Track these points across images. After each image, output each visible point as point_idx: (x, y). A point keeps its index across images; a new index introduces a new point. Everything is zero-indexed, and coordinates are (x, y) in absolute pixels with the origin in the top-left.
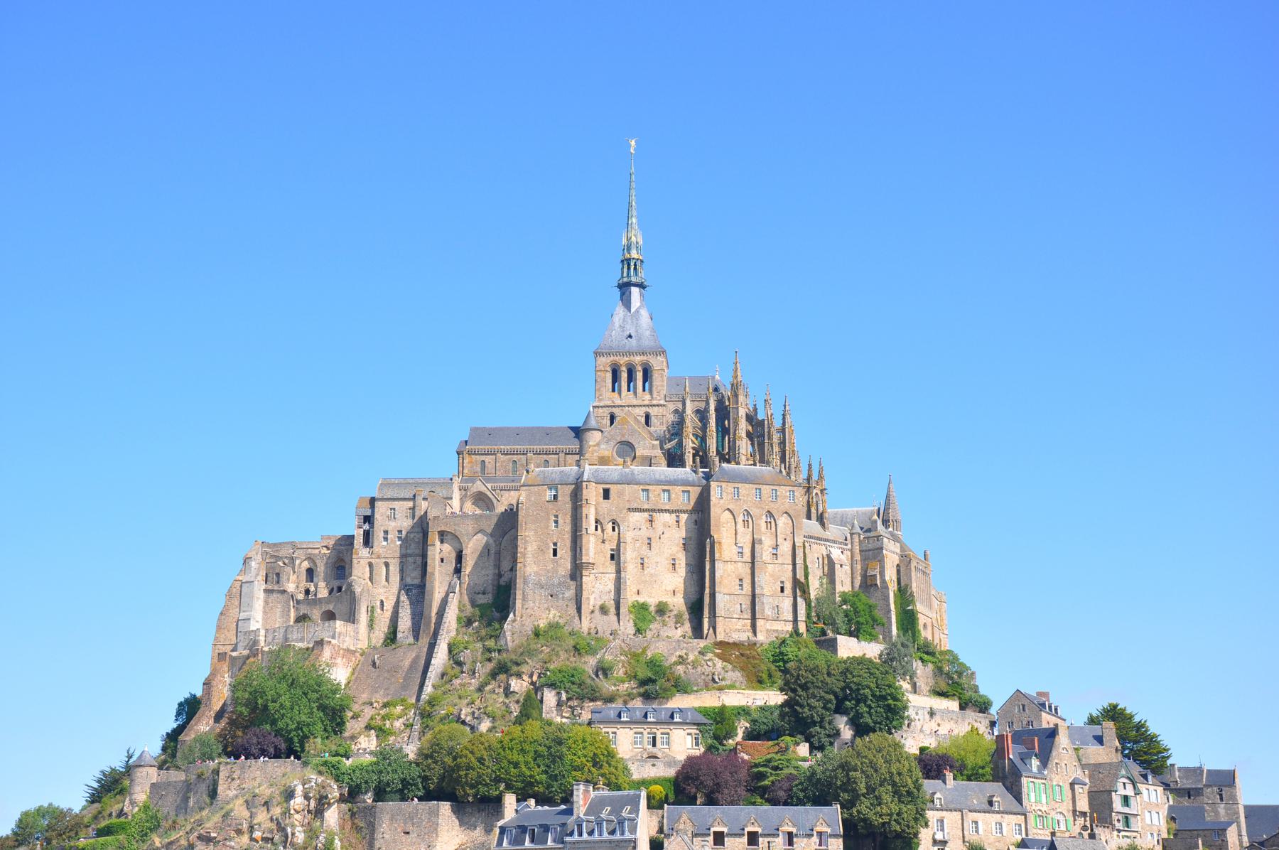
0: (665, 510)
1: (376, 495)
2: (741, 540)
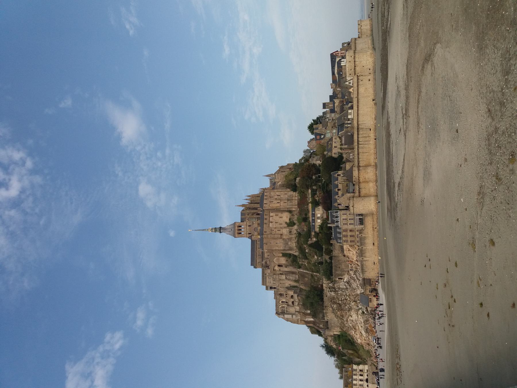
1: (265, 287)
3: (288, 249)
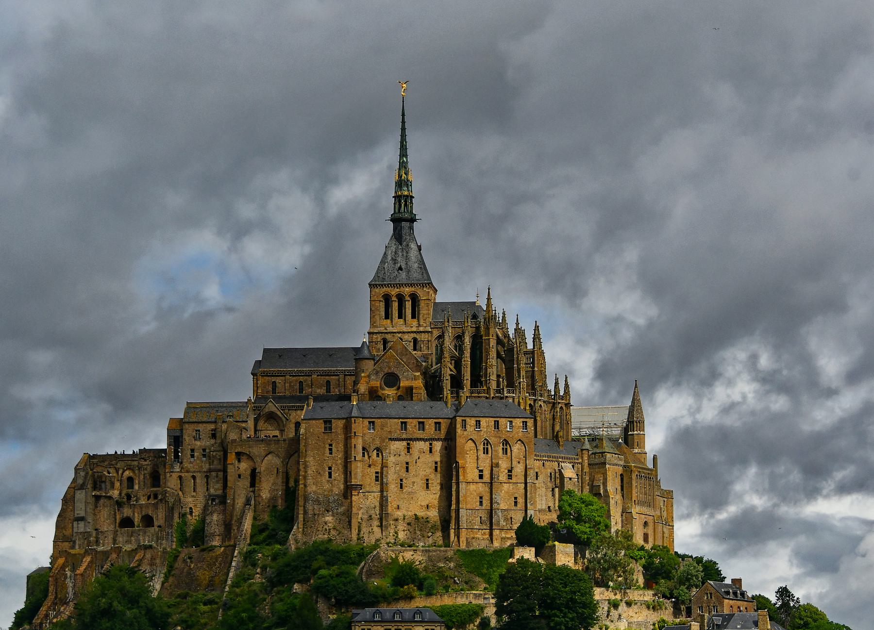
0: (421, 439)
2: (482, 464)
3: (310, 512)
